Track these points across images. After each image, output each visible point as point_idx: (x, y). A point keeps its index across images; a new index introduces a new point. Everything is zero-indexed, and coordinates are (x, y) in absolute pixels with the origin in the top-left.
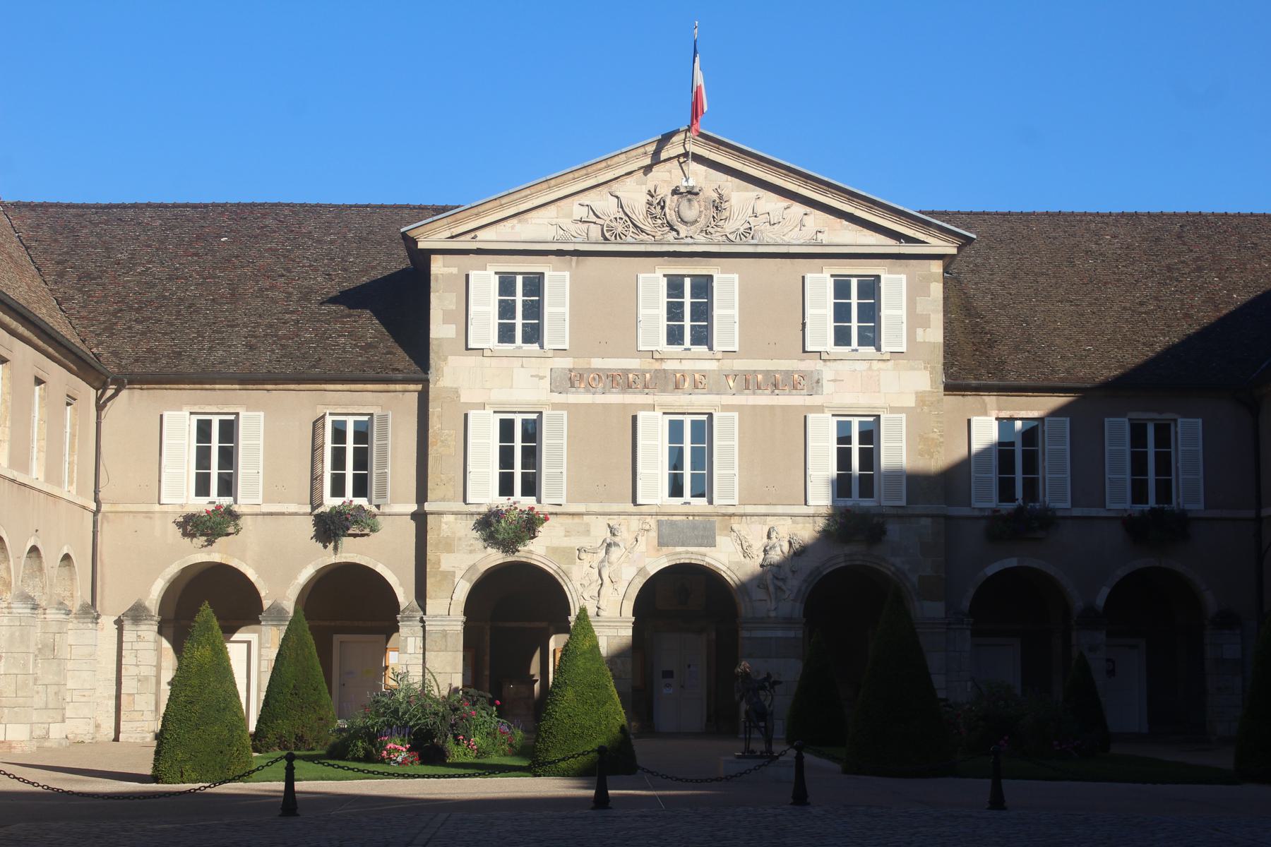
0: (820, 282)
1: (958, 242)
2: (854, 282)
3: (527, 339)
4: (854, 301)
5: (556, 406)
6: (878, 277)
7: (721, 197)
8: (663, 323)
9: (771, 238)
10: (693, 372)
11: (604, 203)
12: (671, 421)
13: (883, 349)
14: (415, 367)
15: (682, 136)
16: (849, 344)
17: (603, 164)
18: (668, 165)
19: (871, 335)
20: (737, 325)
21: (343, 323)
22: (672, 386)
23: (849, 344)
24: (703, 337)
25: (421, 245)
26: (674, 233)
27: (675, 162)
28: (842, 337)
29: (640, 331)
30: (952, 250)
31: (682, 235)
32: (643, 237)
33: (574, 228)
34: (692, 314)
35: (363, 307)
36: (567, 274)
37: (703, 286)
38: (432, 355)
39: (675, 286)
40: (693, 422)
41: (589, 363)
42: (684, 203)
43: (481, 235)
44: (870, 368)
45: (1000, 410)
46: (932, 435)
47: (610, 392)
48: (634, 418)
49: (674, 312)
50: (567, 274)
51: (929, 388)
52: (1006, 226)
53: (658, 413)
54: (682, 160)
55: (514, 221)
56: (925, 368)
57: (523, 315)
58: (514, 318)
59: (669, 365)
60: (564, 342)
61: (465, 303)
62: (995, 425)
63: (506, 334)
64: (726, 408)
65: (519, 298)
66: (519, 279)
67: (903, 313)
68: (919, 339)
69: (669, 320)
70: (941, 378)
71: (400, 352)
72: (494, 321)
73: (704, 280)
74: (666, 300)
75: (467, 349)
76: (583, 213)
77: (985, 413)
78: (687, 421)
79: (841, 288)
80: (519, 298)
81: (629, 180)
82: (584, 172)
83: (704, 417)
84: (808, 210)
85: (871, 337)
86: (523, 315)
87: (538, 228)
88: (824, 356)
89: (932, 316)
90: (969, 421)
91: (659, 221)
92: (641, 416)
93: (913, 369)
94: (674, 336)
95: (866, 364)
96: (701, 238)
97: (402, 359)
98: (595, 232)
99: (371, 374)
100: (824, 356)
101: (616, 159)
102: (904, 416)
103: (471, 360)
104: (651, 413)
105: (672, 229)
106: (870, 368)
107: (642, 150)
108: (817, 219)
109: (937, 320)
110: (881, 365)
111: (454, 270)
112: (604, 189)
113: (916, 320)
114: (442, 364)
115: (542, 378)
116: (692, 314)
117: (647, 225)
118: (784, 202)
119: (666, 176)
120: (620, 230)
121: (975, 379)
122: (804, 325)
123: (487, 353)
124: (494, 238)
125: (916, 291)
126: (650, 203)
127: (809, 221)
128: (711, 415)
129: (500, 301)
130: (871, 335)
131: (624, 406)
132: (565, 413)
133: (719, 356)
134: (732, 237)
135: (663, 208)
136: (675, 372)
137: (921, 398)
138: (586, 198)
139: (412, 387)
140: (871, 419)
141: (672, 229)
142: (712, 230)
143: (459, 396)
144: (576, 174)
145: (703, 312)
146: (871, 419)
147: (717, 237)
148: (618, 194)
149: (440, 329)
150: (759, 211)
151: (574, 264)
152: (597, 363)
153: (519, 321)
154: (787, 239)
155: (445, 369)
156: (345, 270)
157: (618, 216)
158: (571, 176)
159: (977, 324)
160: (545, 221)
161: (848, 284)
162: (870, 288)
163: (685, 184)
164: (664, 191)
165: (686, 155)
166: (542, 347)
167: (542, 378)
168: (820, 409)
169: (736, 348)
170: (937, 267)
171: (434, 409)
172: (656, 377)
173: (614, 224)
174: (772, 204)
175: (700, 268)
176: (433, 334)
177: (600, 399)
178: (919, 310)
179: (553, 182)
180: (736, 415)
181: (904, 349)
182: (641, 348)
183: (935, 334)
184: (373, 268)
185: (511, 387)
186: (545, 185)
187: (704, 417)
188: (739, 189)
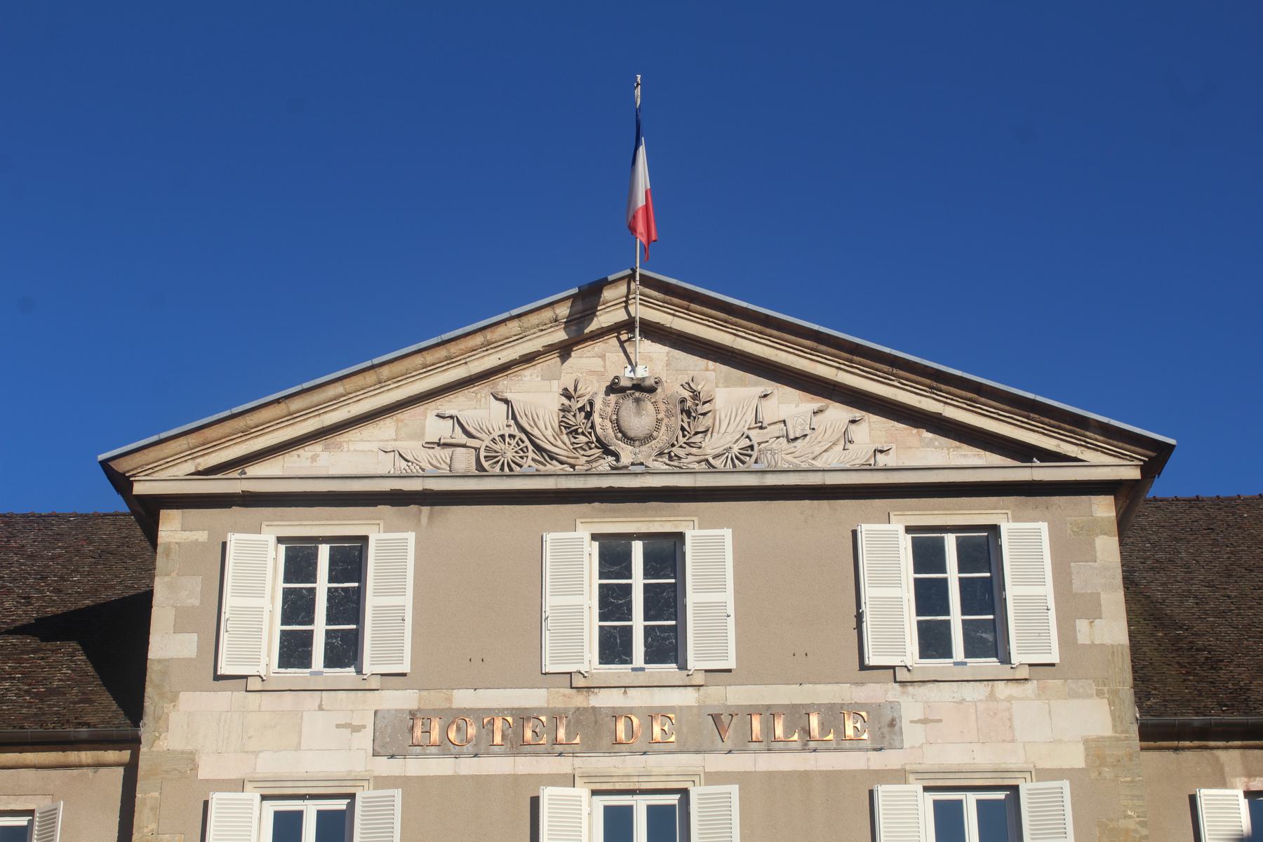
0: (887, 540)
1: (1142, 456)
2: (950, 541)
3: (333, 659)
4: (953, 574)
5: (382, 782)
6: (994, 530)
7: (696, 396)
8: (592, 624)
9: (786, 462)
10: (651, 715)
11: (479, 410)
12: (607, 808)
13: (1015, 659)
14: (122, 719)
15: (622, 289)
16: (948, 654)
17: (478, 340)
18: (599, 346)
19: (989, 636)
20: (731, 622)
21: (19, 661)
22: (606, 741)
23: (948, 654)
24: (666, 647)
25: (138, 489)
26: (610, 459)
27: (613, 342)
28: (933, 641)
29: (547, 636)
30: (1135, 474)
31: (626, 459)
32: (555, 467)
33: (425, 458)
34: (646, 608)
35: (69, 639)
36: (411, 536)
37: (667, 554)
38: (149, 690)
39: (613, 555)
40: (651, 809)
41: (450, 700)
42: (628, 406)
43: (253, 470)
44: (992, 696)
45: (1250, 775)
46: (1123, 823)
47: (489, 754)
48: (535, 802)
49: (613, 603)
50: (411, 536)
51: (1107, 731)
52: (1196, 513)
53: (582, 791)
54: (624, 337)
55: (316, 448)
56: (1100, 694)
57: (326, 618)
58: (311, 622)
59: (603, 700)
60: (400, 661)
61: (224, 592)
62: (1244, 805)
63: (294, 651)
64: (714, 778)
65: (322, 585)
66: (324, 551)
67: (1047, 590)
68: (1083, 639)
69: (603, 617)
70: (1131, 712)
71: (107, 699)
72: (272, 627)
73: (667, 544)
74: (597, 581)
75: (218, 678)
76: (444, 430)
77: (1221, 781)
78: (640, 806)
79: (927, 554)
80: (322, 585)
81: (530, 376)
82: (442, 353)
83: (673, 800)
84: (858, 414)
85: (989, 640)
86: (326, 618)
87: (362, 457)
88: (902, 675)
89: (1103, 596)
90: (1193, 800)
91: (582, 439)
92: (548, 795)
93: (1073, 695)
94: (614, 647)
95: (981, 690)
96: (659, 465)
97: (105, 707)
98: (464, 460)
99: (32, 729)
100: (902, 675)
101: (502, 331)
102: (1066, 785)
103: (224, 698)
104: (568, 791)
105: (607, 451)
106: (992, 696)
107: (547, 314)
108: (873, 430)
109: (1114, 602)
110: (1013, 689)
111: (202, 536)
112: (483, 390)
113: (1073, 605)
114: (168, 707)
115: (357, 729)
116: (646, 608)
117: (561, 446)
118: (818, 403)
119: (596, 364)
120: (510, 455)
121: (1197, 714)
122: (859, 617)
123: (254, 684)
124: (279, 473)
125: (1067, 553)
126: (565, 410)
127: (859, 433)
128: (685, 793)
129: (287, 593)
130: (989, 636)
131: (515, 779)
132: (398, 793)
133: (699, 679)
134: (718, 463)
135: (589, 415)
136: (615, 715)
137: (1094, 748)
138: (450, 405)
139: (111, 755)
140: (1000, 796)
141: (607, 451)
142: (681, 453)
143: (195, 768)
144: (430, 357)
145: (667, 601)
146: (1000, 796)
147: (690, 463)
148: (509, 396)
149: (167, 643)
150: (768, 415)
151: (424, 520)
152: (464, 698)
153: (320, 627)
154: (819, 464)
155: (174, 717)
156: (58, 591)
157: (507, 432)
158: (418, 360)
159: (1179, 639)
160: (375, 446)
161: (939, 548)
162: (982, 550)
163: (628, 374)
164: (594, 388)
165: (628, 325)
166: (359, 672)
167: (357, 729)
168: (900, 776)
169: (731, 664)
170: (1104, 508)
171: (146, 794)
172: (578, 722)
173: (499, 446)
174: (790, 405)
175: (659, 520)
176: (151, 655)
177: (469, 766)
178: (1077, 586)
179: (385, 372)
180: (734, 789)
181: (1054, 658)
182: (549, 668)
183: (1111, 628)
184: (112, 587)
185: (298, 748)
186: (370, 378)
187: (673, 800)
188: (728, 383)
